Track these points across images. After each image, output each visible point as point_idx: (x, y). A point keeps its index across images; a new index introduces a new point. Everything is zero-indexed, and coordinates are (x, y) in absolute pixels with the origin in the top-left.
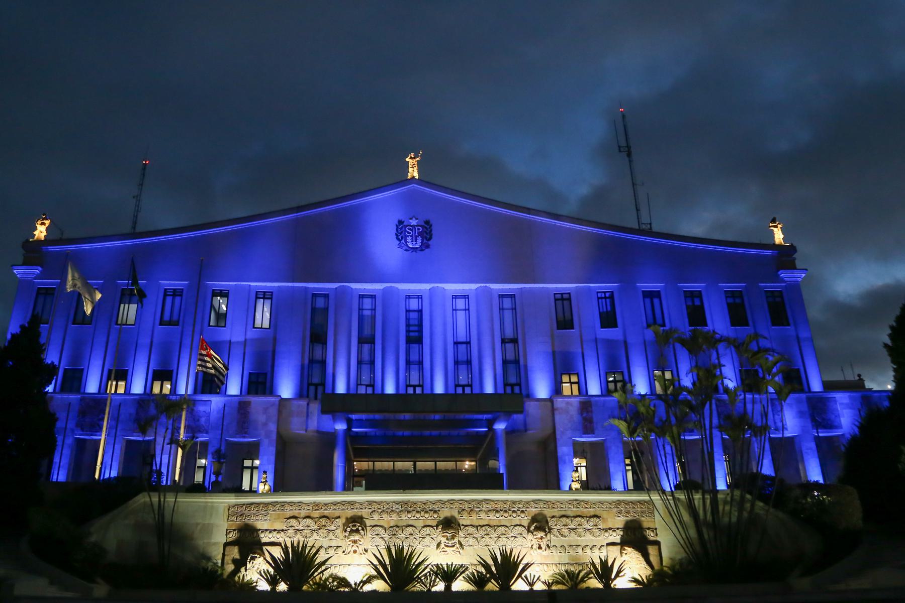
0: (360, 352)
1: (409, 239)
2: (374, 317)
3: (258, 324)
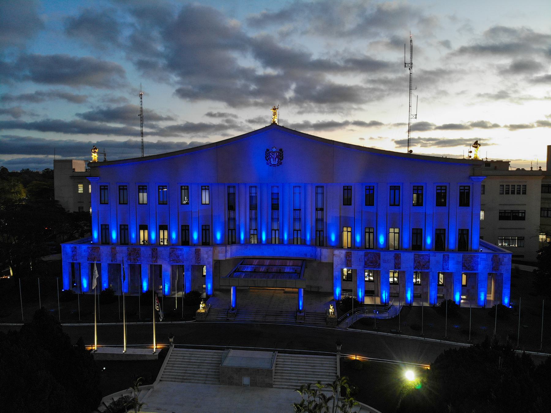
0: (250, 213)
1: (272, 159)
2: (256, 196)
3: (204, 202)
